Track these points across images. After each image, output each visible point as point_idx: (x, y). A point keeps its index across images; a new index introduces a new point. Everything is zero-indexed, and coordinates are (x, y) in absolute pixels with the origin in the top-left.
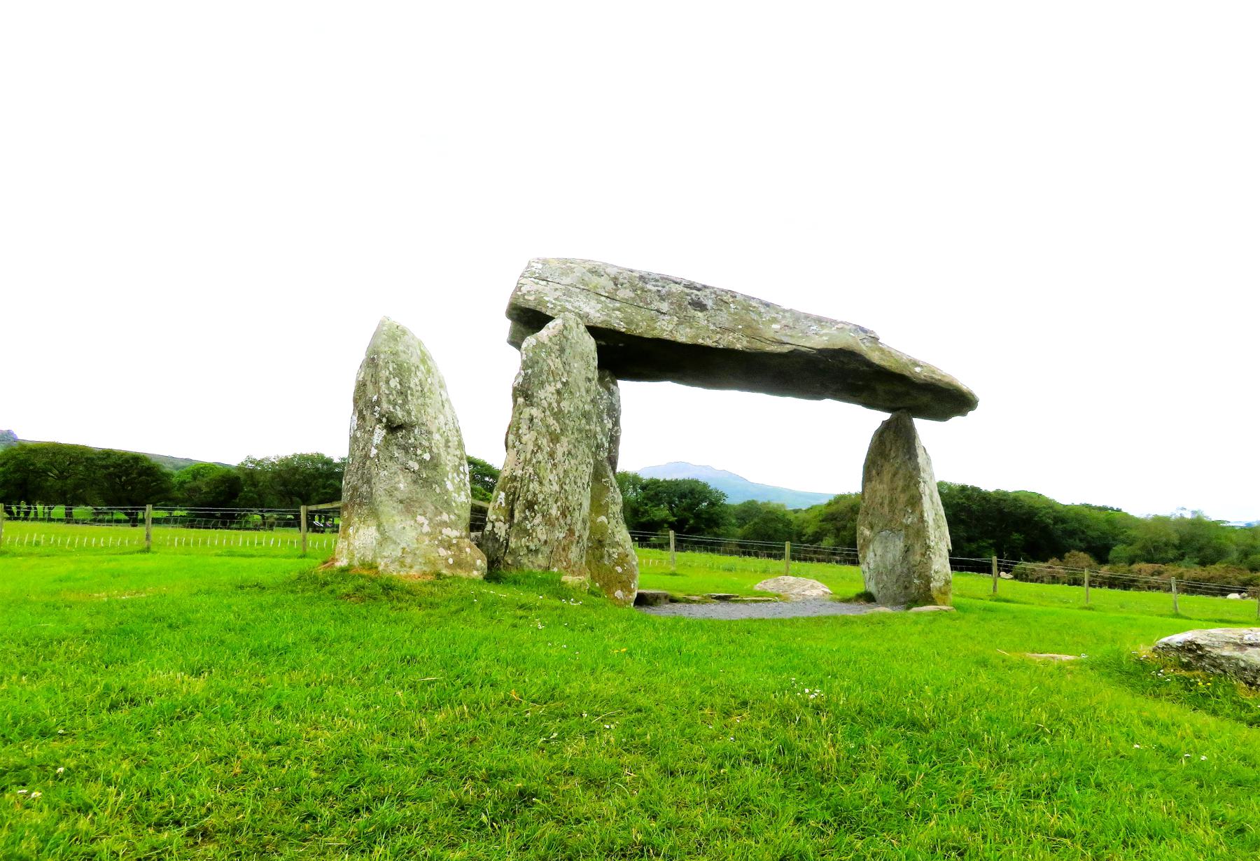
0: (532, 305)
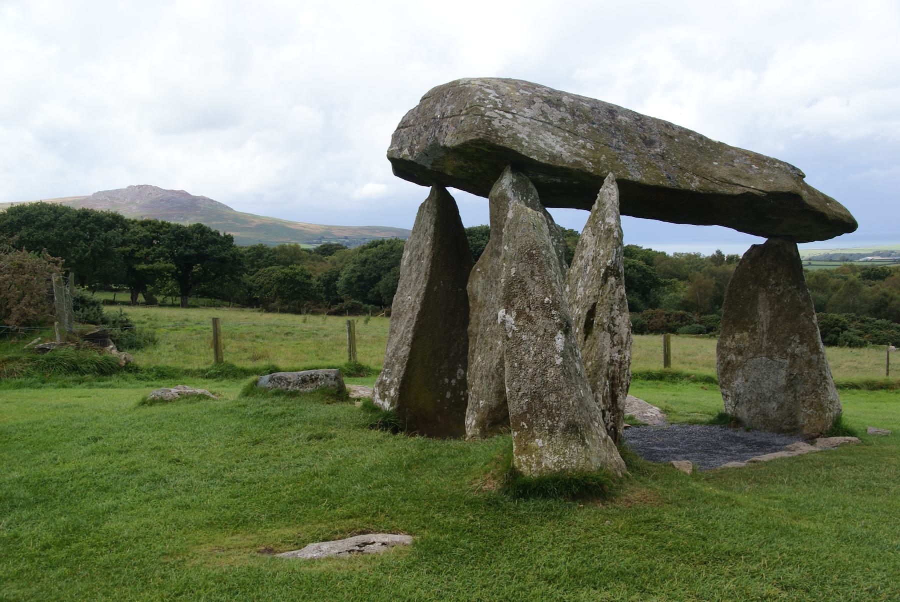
0: (508, 143)
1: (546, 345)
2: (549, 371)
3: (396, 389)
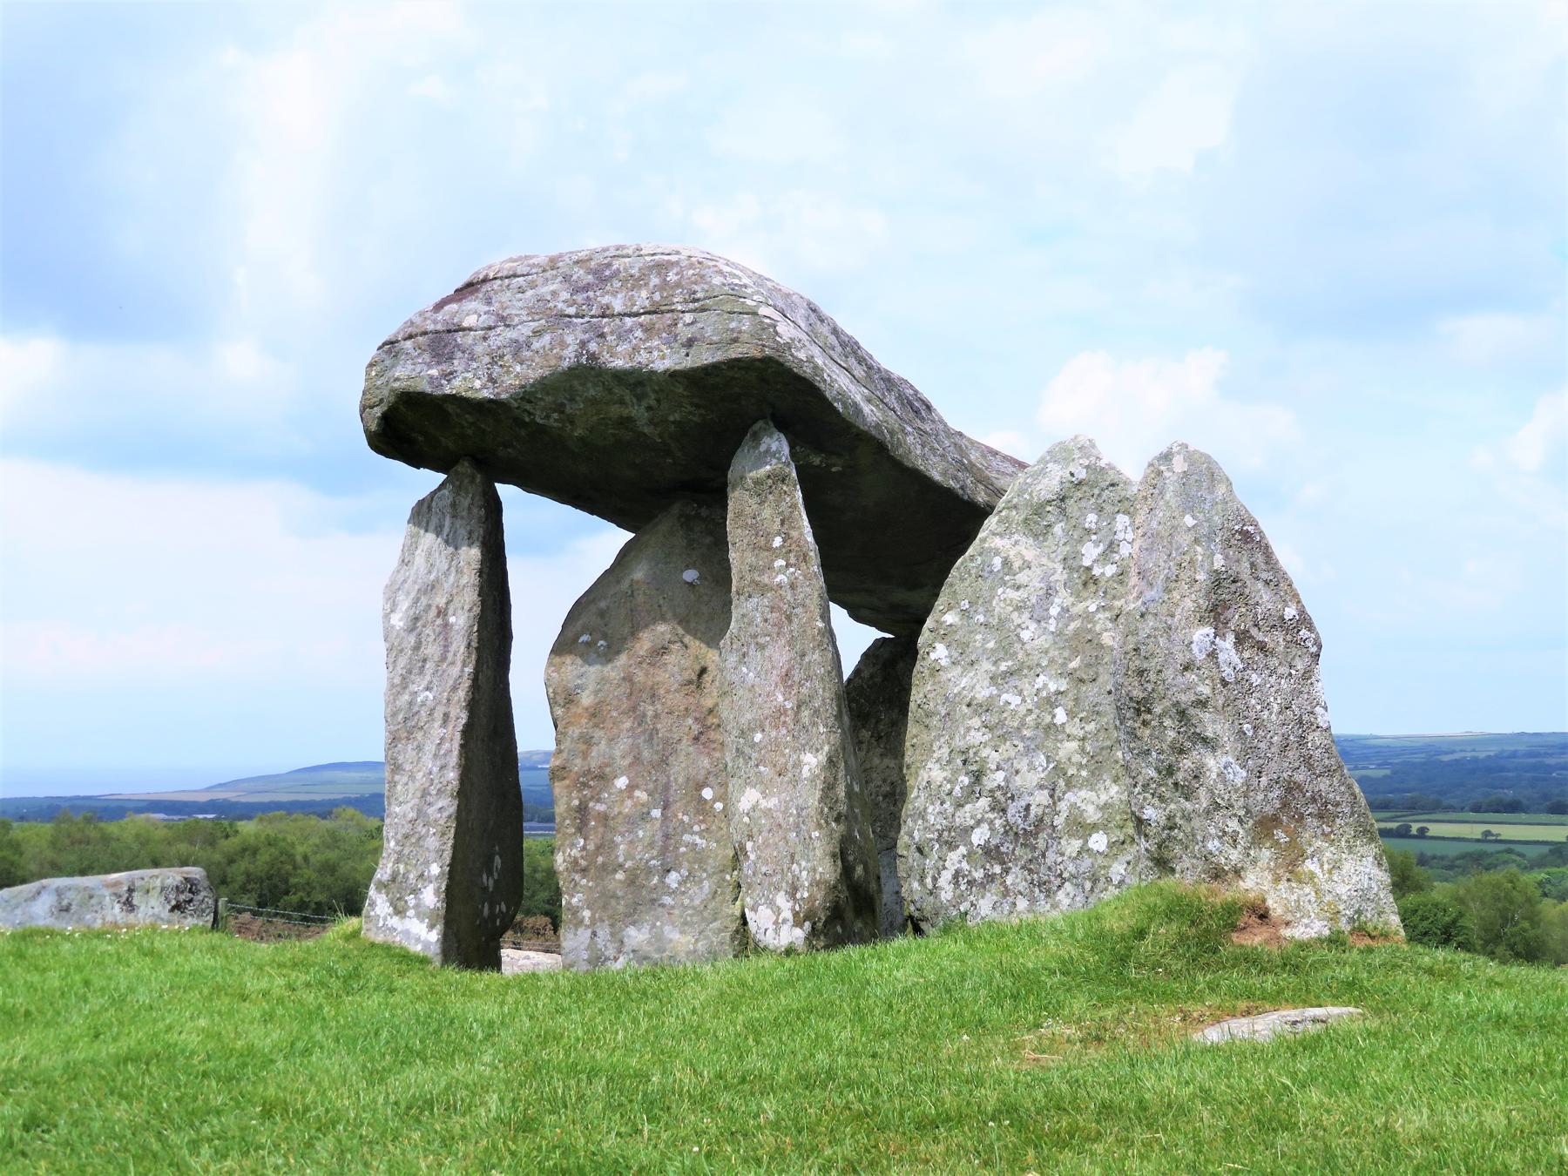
0: (807, 371)
1: (1296, 693)
2: (1310, 738)
3: (437, 892)
